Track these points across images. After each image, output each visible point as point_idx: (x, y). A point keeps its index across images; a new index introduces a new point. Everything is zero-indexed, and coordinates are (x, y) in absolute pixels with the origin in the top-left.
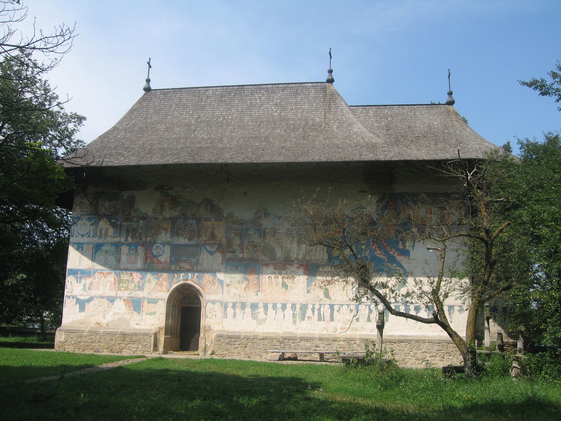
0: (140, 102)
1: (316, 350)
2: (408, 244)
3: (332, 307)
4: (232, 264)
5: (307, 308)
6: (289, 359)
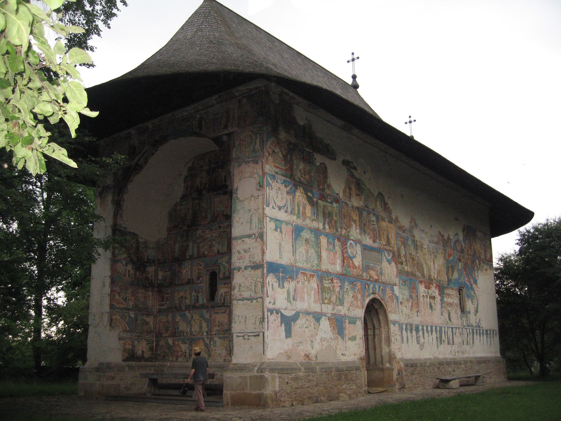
2: (476, 274)
3: (452, 328)
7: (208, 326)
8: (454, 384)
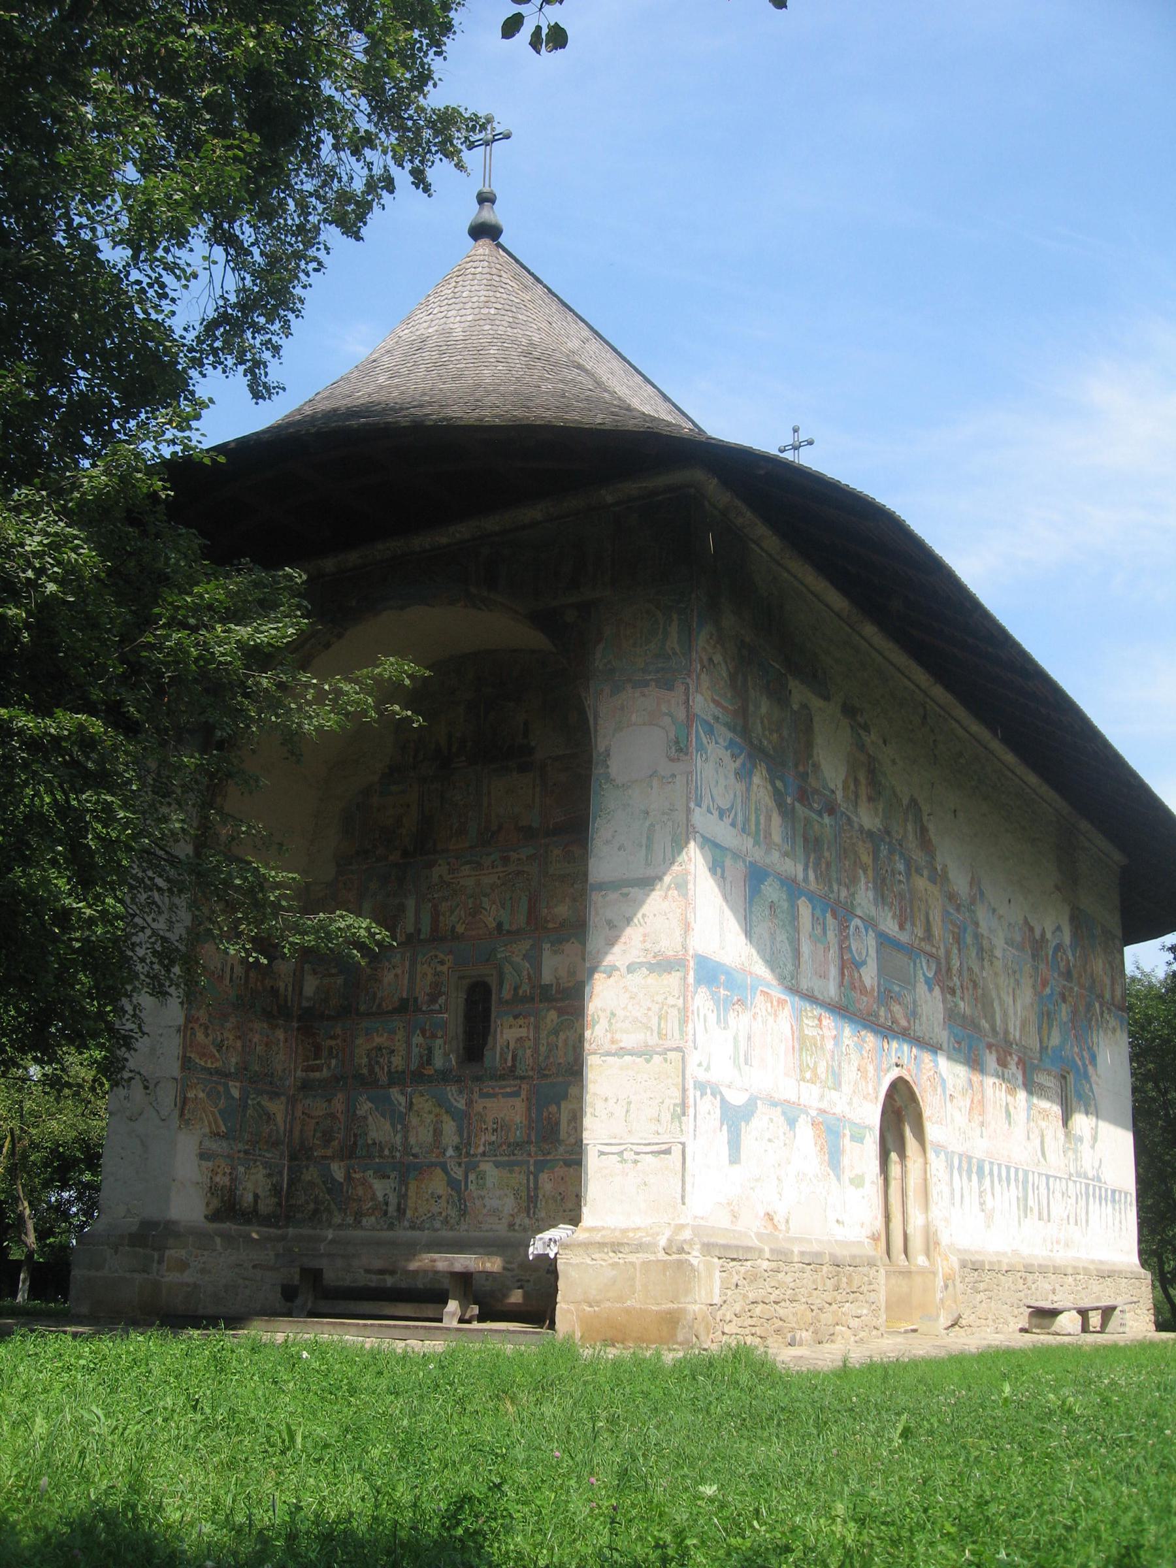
2: (1095, 1040)
7: (460, 1131)
8: (1068, 1322)
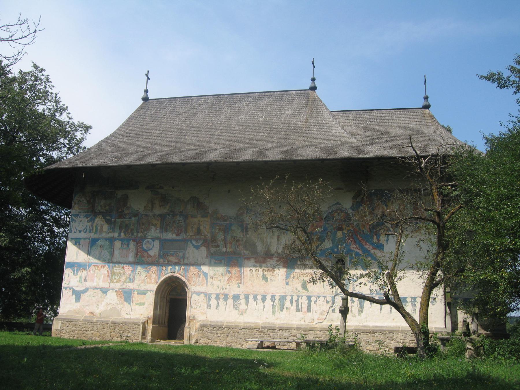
0: (138, 110)
1: (293, 340)
2: (382, 238)
3: (309, 298)
4: (216, 258)
5: (286, 299)
6: (268, 347)
